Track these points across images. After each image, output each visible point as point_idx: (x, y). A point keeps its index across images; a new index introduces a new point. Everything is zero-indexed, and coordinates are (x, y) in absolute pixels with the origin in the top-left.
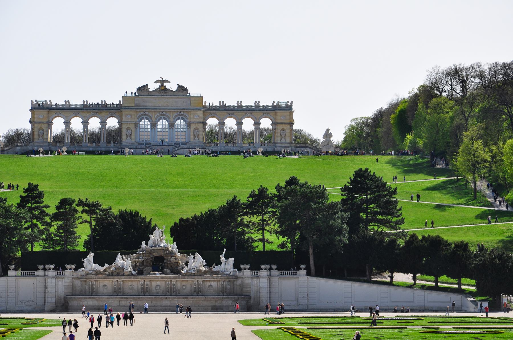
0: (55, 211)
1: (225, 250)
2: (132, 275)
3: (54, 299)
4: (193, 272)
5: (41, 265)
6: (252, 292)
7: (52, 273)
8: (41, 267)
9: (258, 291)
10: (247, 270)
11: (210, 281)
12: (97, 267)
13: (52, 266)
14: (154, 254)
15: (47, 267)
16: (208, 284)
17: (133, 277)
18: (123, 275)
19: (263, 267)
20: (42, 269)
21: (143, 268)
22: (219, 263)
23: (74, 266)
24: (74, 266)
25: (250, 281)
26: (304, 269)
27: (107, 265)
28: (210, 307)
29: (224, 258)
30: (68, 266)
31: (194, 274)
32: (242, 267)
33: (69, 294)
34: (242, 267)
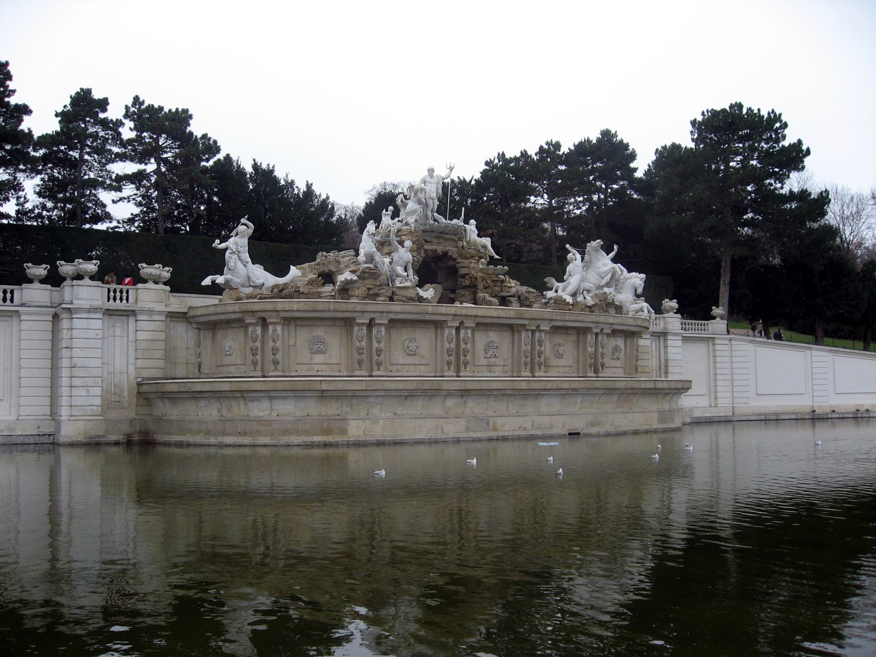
0: (53, 126)
1: (615, 247)
3: (98, 391)
4: (590, 301)
5: (37, 262)
7: (88, 294)
8: (41, 271)
12: (261, 275)
13: (91, 267)
14: (426, 247)
15: (66, 268)
18: (391, 299)
20: (43, 281)
23: (166, 273)
24: (166, 273)
26: (722, 318)
27: (294, 271)
28: (656, 415)
30: (146, 269)
31: (591, 308)
33: (153, 373)
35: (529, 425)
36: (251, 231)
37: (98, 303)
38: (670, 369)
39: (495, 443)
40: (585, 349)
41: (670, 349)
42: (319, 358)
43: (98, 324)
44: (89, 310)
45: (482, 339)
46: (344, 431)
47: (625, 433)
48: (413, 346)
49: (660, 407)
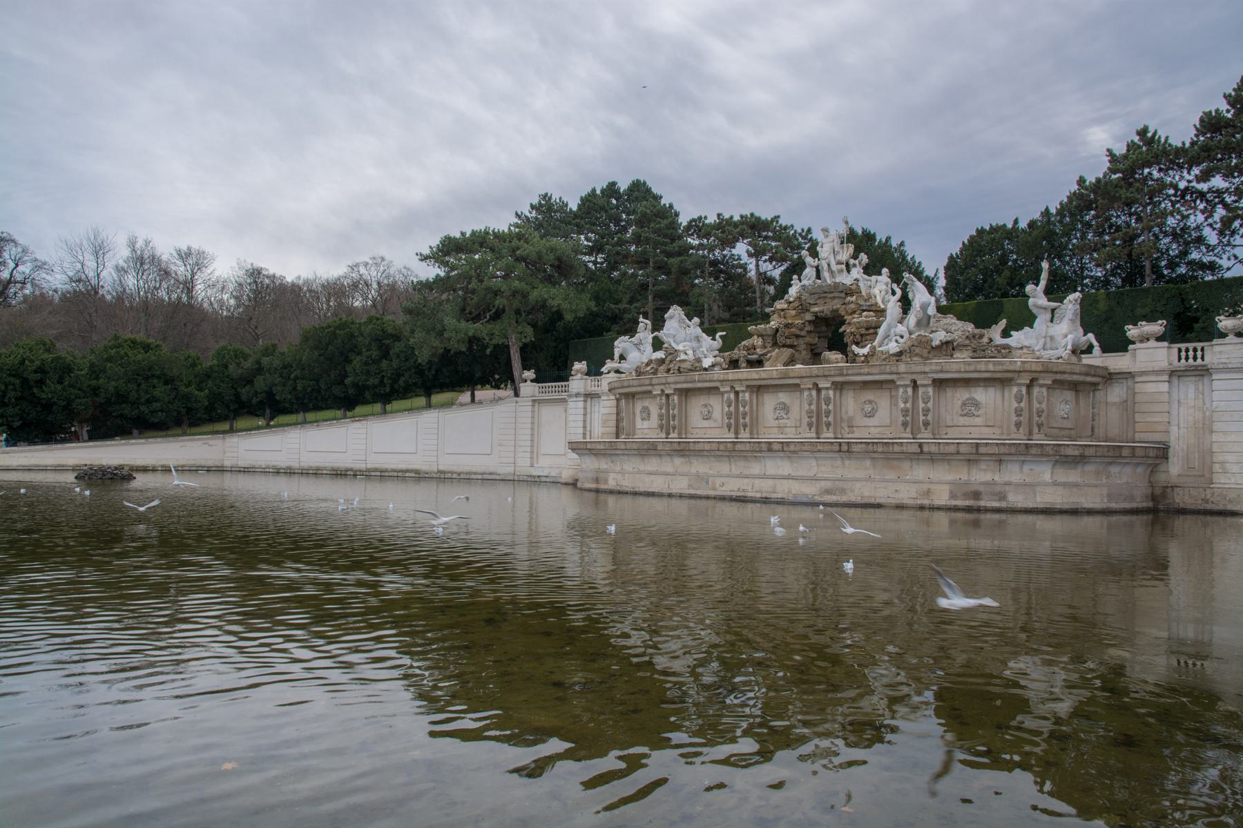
1: (1045, 265)
2: (706, 369)
4: (893, 347)
6: (1174, 429)
9: (1206, 427)
10: (1152, 343)
11: (967, 382)
16: (962, 394)
17: (696, 376)
19: (1224, 323)
21: (765, 354)
22: (1025, 319)
25: (1164, 387)
29: (1043, 301)
31: (900, 354)
32: (1132, 331)
34: (1132, 331)
35: (749, 488)
36: (650, 327)
37: (582, 391)
38: (1216, 426)
39: (711, 502)
40: (896, 405)
41: (1216, 395)
42: (646, 424)
43: (581, 404)
44: (577, 395)
45: (770, 402)
46: (606, 481)
47: (879, 506)
48: (705, 411)
49: (965, 477)
